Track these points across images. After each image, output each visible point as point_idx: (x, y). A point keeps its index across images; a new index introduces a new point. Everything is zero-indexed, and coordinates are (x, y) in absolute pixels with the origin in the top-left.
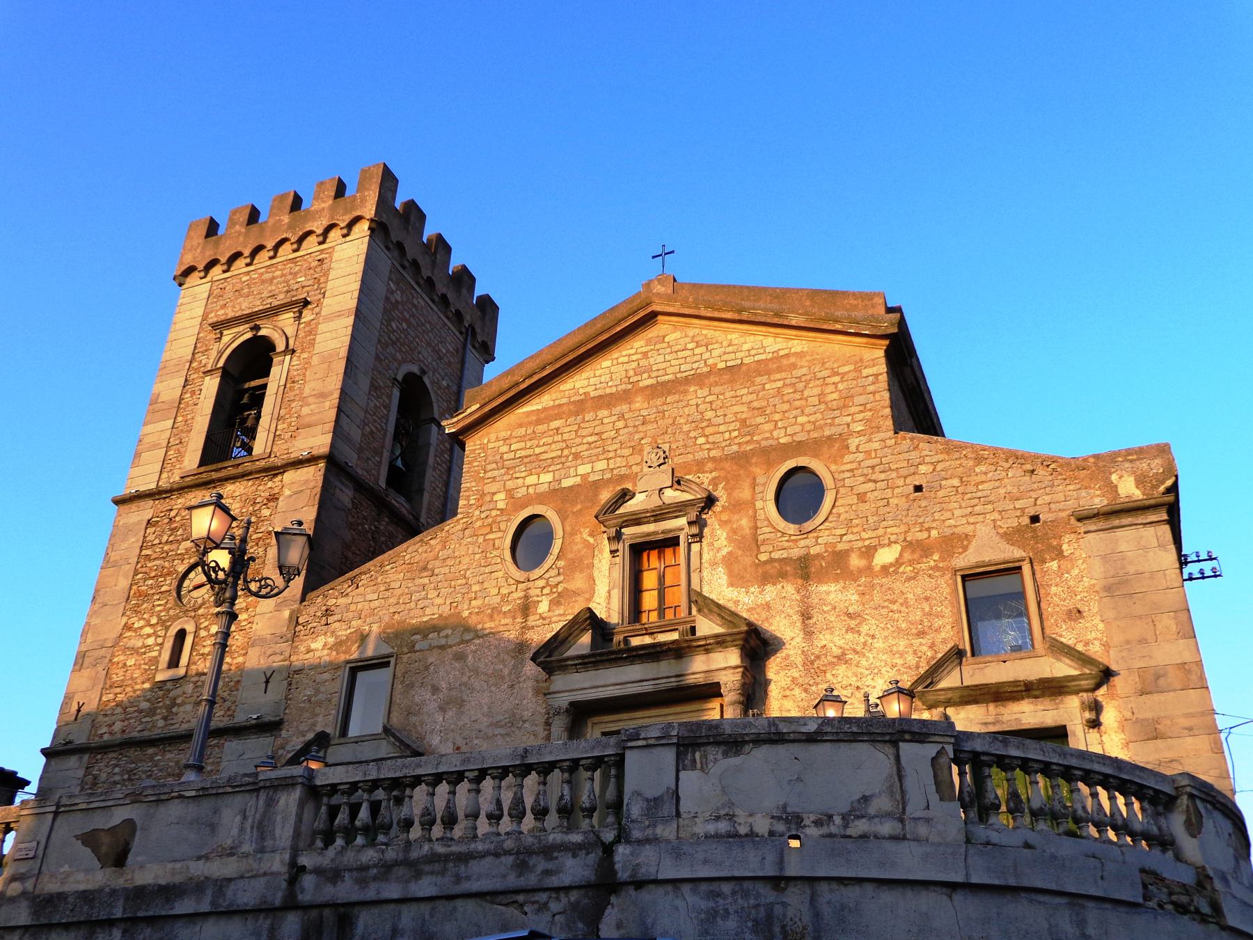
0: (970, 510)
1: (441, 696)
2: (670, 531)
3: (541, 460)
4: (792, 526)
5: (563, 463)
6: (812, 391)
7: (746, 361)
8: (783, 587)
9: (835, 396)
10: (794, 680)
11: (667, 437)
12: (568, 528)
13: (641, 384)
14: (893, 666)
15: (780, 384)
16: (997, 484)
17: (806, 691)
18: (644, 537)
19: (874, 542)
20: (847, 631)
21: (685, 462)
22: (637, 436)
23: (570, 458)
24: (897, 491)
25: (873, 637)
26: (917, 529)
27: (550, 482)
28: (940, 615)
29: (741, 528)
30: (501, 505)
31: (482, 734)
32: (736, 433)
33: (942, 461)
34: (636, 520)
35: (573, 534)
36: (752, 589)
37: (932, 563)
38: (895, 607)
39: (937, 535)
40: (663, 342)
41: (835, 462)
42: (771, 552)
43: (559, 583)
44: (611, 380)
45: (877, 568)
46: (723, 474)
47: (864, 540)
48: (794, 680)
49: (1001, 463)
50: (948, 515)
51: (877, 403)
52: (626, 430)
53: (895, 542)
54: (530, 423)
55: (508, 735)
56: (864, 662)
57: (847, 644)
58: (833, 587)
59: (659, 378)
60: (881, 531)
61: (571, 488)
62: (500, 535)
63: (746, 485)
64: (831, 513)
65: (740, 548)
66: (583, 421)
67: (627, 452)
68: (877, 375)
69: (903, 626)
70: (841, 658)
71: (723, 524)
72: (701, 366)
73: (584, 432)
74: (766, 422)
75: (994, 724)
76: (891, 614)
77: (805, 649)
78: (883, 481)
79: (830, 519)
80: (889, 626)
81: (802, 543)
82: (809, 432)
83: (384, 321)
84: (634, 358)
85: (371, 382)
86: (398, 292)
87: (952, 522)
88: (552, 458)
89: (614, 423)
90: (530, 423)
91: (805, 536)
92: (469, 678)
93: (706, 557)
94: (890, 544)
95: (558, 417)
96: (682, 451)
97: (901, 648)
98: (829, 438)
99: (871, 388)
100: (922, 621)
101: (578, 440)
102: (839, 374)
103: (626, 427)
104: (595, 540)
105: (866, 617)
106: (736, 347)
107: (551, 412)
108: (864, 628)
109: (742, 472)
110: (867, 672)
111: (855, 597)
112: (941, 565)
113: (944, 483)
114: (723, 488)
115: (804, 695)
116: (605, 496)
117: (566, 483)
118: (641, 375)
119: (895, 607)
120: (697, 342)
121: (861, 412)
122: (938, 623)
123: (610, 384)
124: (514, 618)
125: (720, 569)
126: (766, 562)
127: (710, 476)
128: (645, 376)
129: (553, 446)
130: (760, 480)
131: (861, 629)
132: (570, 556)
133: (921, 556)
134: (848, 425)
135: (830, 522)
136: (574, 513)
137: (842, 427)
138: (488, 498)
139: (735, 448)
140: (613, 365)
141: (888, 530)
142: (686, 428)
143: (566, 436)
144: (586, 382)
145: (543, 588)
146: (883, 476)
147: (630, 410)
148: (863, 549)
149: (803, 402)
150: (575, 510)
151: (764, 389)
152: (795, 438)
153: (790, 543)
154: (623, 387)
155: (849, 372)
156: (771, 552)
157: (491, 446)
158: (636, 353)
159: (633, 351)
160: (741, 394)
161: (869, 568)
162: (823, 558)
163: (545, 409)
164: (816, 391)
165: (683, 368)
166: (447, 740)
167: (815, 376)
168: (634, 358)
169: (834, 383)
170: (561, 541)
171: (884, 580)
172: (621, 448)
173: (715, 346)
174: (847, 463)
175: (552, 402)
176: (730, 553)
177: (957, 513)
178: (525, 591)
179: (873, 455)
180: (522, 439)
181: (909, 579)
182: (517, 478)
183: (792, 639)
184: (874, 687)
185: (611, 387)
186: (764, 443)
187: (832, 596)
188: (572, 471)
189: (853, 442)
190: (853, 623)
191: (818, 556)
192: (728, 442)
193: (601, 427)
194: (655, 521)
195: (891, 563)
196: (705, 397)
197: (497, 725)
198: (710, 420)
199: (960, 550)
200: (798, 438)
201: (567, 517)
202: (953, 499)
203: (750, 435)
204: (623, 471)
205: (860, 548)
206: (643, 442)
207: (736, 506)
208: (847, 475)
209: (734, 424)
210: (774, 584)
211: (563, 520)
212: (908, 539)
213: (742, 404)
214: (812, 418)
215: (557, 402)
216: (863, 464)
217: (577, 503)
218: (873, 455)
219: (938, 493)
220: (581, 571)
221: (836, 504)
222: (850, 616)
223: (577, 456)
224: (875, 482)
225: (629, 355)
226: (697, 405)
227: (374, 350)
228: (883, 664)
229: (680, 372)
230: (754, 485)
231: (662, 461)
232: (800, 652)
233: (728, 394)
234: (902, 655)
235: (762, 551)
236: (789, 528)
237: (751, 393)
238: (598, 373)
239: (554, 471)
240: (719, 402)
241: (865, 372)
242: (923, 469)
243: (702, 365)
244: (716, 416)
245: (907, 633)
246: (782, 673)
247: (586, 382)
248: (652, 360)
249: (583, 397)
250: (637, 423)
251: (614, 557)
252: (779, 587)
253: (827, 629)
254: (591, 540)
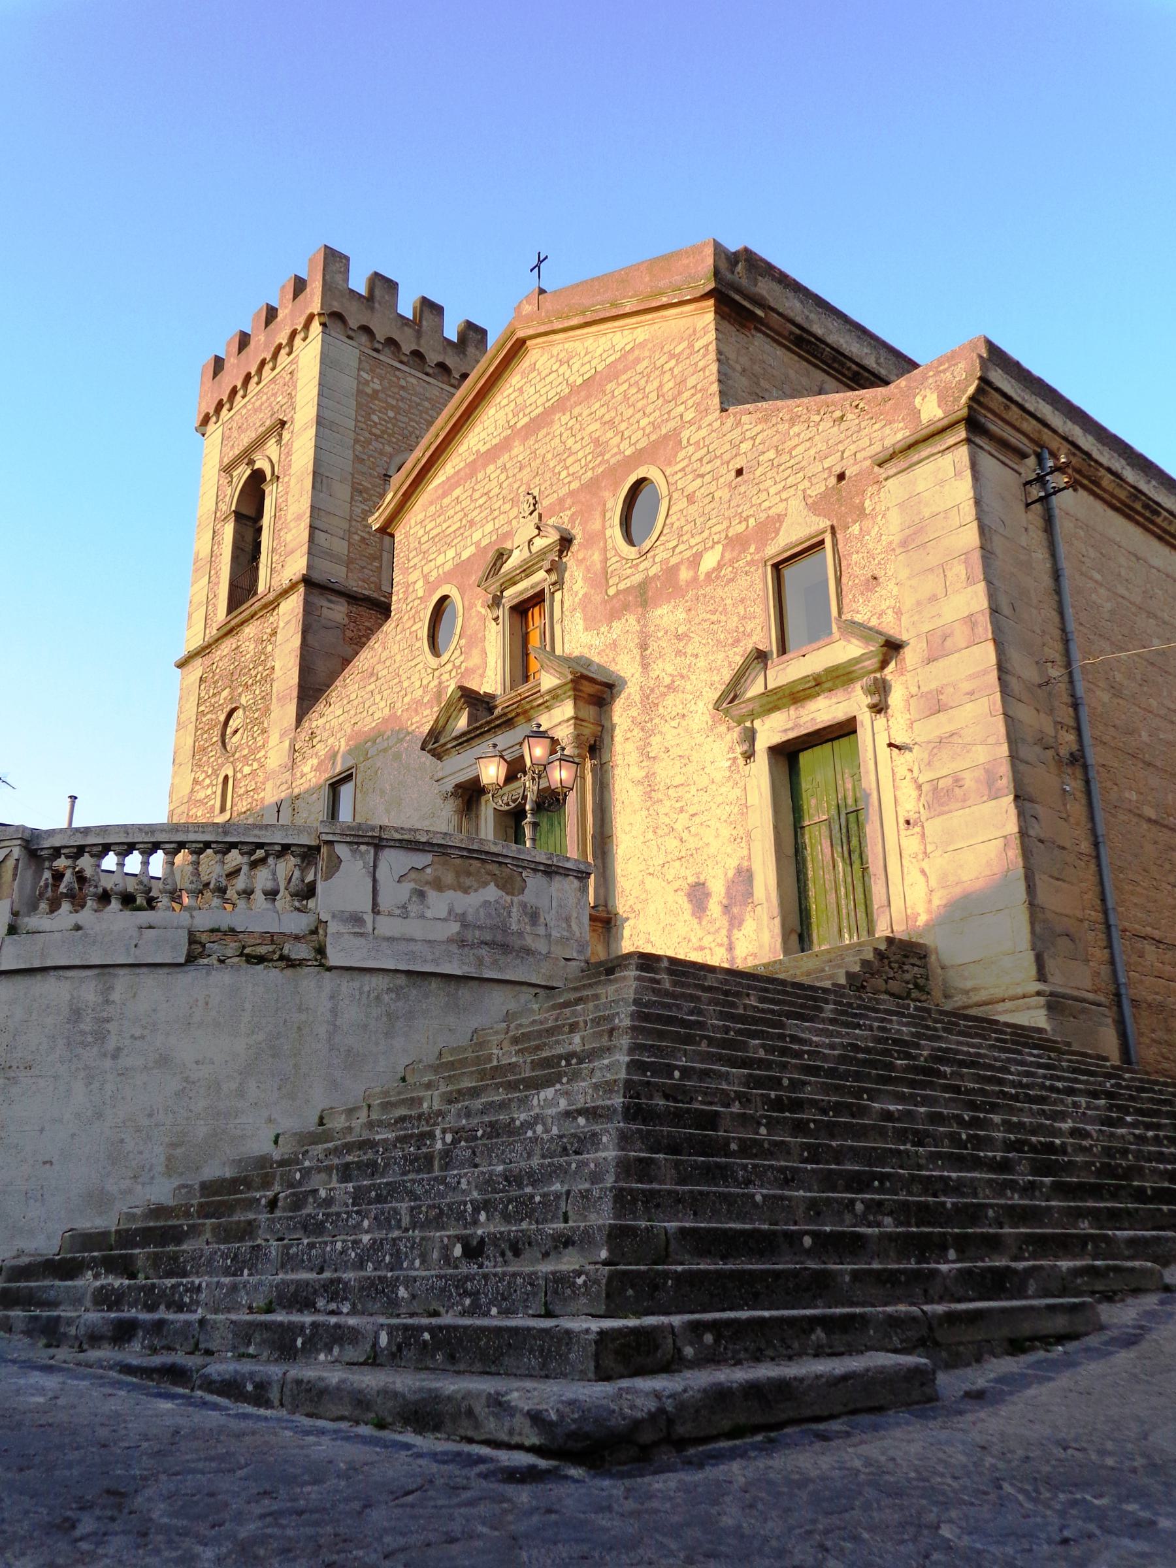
2: (538, 584)
12: (466, 603)
24: (722, 480)
30: (420, 593)
36: (602, 629)
47: (691, 547)
64: (665, 524)
66: (477, 482)
67: (507, 507)
69: (722, 637)
71: (580, 562)
75: (792, 729)
83: (359, 418)
85: (352, 487)
86: (375, 380)
95: (457, 485)
111: (683, 615)
113: (761, 458)
117: (465, 555)
122: (750, 626)
124: (432, 708)
127: (569, 513)
133: (740, 553)
138: (411, 589)
139: (590, 474)
157: (412, 532)
159: (511, 390)
161: (695, 578)
163: (448, 479)
176: (585, 595)
180: (433, 518)
194: (527, 576)
212: (730, 535)
224: (702, 476)
227: (351, 452)
231: (532, 508)
242: (744, 447)
252: (623, 621)
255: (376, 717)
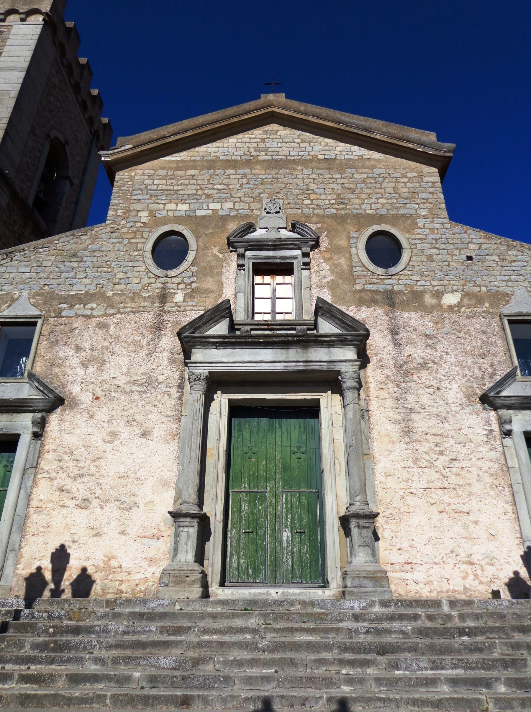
0: (507, 277)
1: (84, 354)
3: (179, 194)
4: (379, 269)
5: (197, 199)
6: (389, 185)
7: (339, 157)
8: (375, 310)
9: (405, 190)
10: (388, 377)
11: (280, 196)
12: (201, 244)
13: (259, 158)
14: (466, 376)
15: (365, 176)
16: (525, 264)
17: (398, 386)
18: (262, 259)
19: (442, 289)
20: (426, 347)
21: (295, 214)
22: (257, 191)
23: (203, 197)
24: (454, 257)
25: (447, 353)
26: (471, 285)
27: (186, 211)
28: (494, 344)
29: (340, 264)
30: (144, 220)
31: (120, 389)
32: (334, 202)
33: (485, 243)
34: (259, 245)
35: (205, 248)
37: (485, 309)
38: (461, 335)
39: (486, 291)
40: (276, 135)
41: (409, 232)
42: (364, 285)
43: (193, 282)
44: (236, 151)
45: (445, 307)
46: (325, 226)
47: (434, 286)
48: (388, 377)
49: (526, 251)
50: (492, 278)
51: (436, 200)
52: (248, 186)
53: (457, 291)
54: (170, 168)
55: (144, 392)
56: (441, 371)
57: (427, 356)
58: (413, 315)
59: (273, 157)
60: (446, 282)
61: (204, 217)
62: (142, 240)
63: (344, 236)
64: (408, 264)
65: (340, 278)
66: (214, 174)
68: (434, 183)
69: (468, 348)
70: (423, 365)
71: (326, 260)
72: (305, 155)
73: (215, 182)
74: (356, 198)
76: (459, 339)
77: (395, 356)
78: (444, 249)
79: (408, 268)
80: (458, 347)
81: (388, 282)
82: (388, 209)
84: (254, 140)
87: (496, 283)
88: (188, 194)
89: (239, 179)
90: (171, 169)
91: (389, 277)
92: (111, 343)
93: (314, 281)
94: (453, 291)
95: (194, 168)
96: (292, 206)
97: (469, 364)
98: (403, 216)
99: (431, 190)
100: (481, 346)
101: (210, 186)
102: (407, 177)
103: (248, 183)
104: (224, 256)
105: (440, 338)
106: (331, 148)
107: (188, 164)
108: (439, 347)
109: (340, 227)
110: (444, 378)
111: (430, 324)
112: (491, 311)
113: (488, 257)
114: (326, 236)
115: (396, 389)
116: (232, 227)
117: (199, 213)
118: (260, 152)
119: (461, 335)
120: (302, 140)
121: (424, 203)
122: (494, 350)
123: (235, 153)
124: (153, 303)
125: (325, 290)
126: (361, 291)
128: (264, 153)
129: (189, 187)
130: (354, 235)
131: (438, 347)
132: (203, 264)
133: (476, 303)
134: (416, 210)
135: (408, 270)
136: (206, 234)
137: (412, 210)
138: (134, 213)
139: (334, 211)
140: (237, 142)
141: (451, 282)
142: (296, 192)
143: (199, 182)
144: (217, 149)
145: (178, 284)
146: (444, 246)
147: (251, 173)
148: (434, 292)
149: (382, 191)
150: (207, 232)
151: (353, 177)
152: (378, 212)
153: (379, 281)
154: (246, 157)
155: (414, 177)
156: (364, 285)
157: (136, 178)
158: (255, 138)
159: (254, 136)
160: (336, 177)
162: (404, 294)
163: (182, 161)
164: (392, 185)
165: (291, 153)
166: (87, 390)
167: (390, 176)
168: (254, 140)
169: (403, 182)
170: (195, 252)
171: (451, 315)
172: (244, 197)
173: (316, 144)
174: (417, 234)
175: (189, 158)
176: (333, 281)
177: (499, 278)
178: (163, 284)
179: (436, 232)
180: (163, 177)
181: (468, 317)
182: (159, 204)
183: (384, 347)
184: (451, 389)
185: (236, 155)
186: (355, 211)
187: (413, 321)
188: (205, 206)
189: (421, 222)
190: (431, 342)
191: (400, 292)
192: (328, 206)
193: (228, 180)
194: (274, 250)
195: (455, 305)
196: (309, 175)
197: (135, 383)
198: (313, 190)
199: (504, 303)
200: (381, 212)
201: (201, 236)
202: (496, 268)
203: (344, 204)
204: (246, 212)
205: (431, 291)
206: (261, 195)
207: (335, 249)
208: (419, 241)
209: (332, 195)
210: (368, 307)
211: (197, 238)
212: (465, 290)
213: (337, 184)
214: (390, 201)
215: (193, 158)
216: (428, 237)
217: (209, 228)
218: (436, 232)
219: (484, 263)
220: (212, 276)
221: (412, 259)
222: (428, 336)
223: (208, 196)
224: (438, 249)
225: (250, 138)
226: (303, 179)
228: (456, 373)
229: (290, 155)
230: (349, 237)
231: (278, 209)
232: (391, 357)
233: (327, 176)
234: (470, 369)
235: (357, 282)
236: (378, 270)
237: (344, 178)
238: (225, 145)
239: (190, 203)
240: (320, 180)
241: (425, 179)
242: (471, 246)
243: (307, 154)
244: (318, 188)
245: (471, 353)
246: (378, 371)
247: (217, 149)
248: (268, 145)
249: (214, 158)
250: (256, 183)
251: (240, 270)
252: (372, 309)
253: (412, 343)
254: (221, 256)
255: (75, 287)
